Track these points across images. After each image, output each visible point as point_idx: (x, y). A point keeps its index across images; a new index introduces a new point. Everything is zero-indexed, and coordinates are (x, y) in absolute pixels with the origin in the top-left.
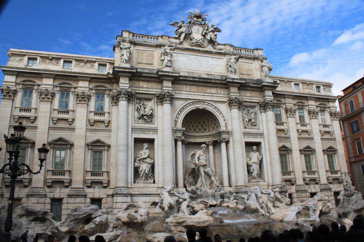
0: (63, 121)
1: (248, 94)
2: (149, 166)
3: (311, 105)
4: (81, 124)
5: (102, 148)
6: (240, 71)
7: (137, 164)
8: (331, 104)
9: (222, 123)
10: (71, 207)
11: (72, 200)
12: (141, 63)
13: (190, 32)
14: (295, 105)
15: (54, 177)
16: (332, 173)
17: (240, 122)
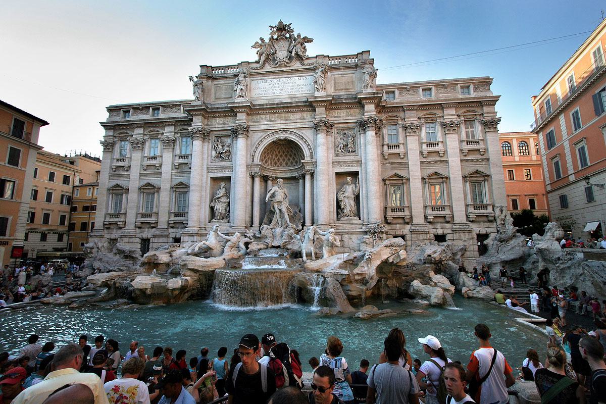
0: (152, 167)
1: (343, 113)
2: (224, 205)
3: (448, 115)
4: (167, 169)
5: (186, 190)
6: (335, 86)
7: (212, 204)
8: (486, 109)
9: (306, 152)
10: (155, 246)
11: (156, 240)
12: (219, 99)
13: (274, 51)
14: (419, 118)
15: (143, 219)
16: (475, 208)
17: (328, 149)
